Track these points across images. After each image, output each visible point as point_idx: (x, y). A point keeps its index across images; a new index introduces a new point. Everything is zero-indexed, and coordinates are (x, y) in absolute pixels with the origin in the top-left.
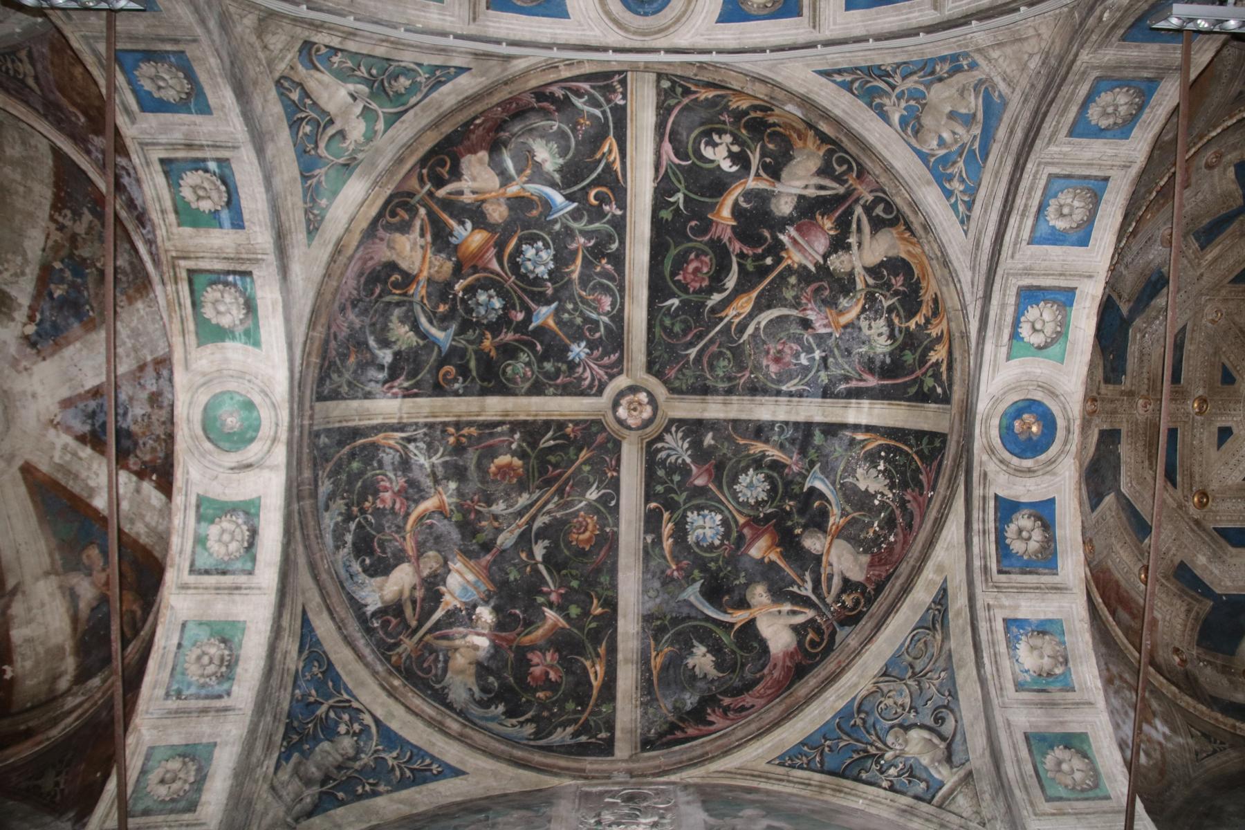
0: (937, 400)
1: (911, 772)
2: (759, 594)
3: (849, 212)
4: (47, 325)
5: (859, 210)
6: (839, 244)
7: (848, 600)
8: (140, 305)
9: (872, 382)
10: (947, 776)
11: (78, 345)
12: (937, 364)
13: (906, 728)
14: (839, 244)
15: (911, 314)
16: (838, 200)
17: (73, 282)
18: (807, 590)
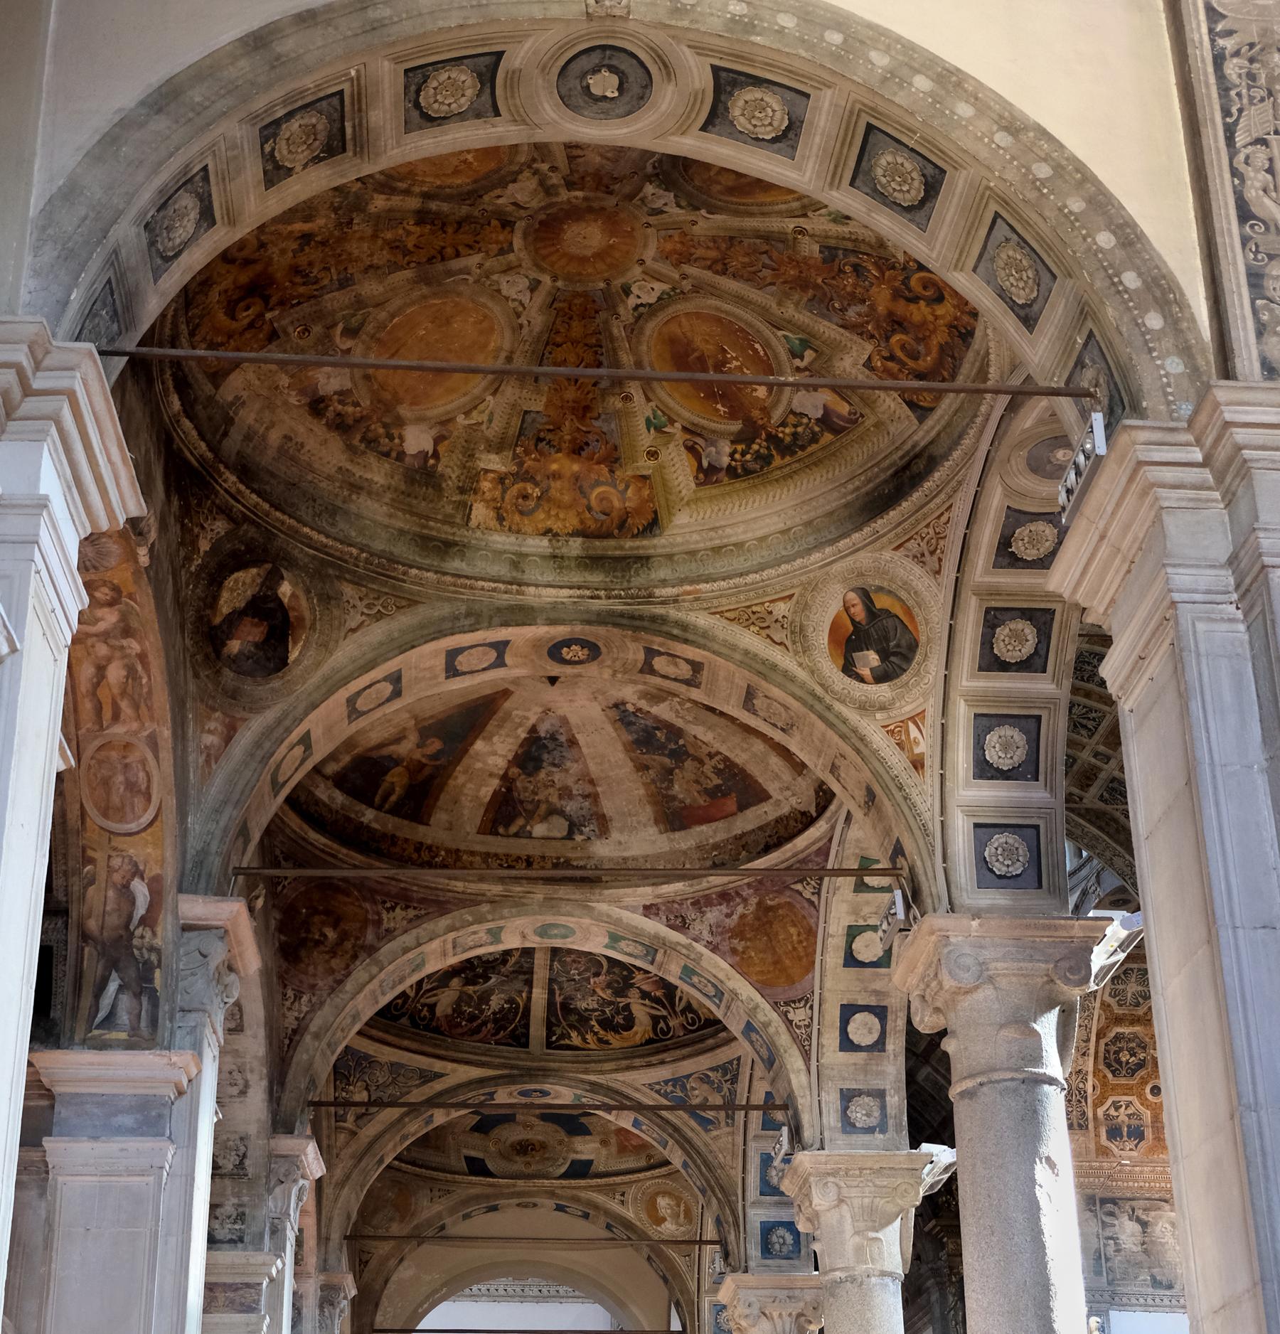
0: (548, 1037)
3: (664, 1007)
4: (633, 719)
5: (664, 1013)
6: (645, 995)
7: (425, 1012)
8: (642, 792)
9: (558, 999)
11: (614, 734)
12: (570, 1037)
13: (367, 1089)
14: (645, 995)
15: (600, 1023)
16: (673, 1005)
17: (666, 748)
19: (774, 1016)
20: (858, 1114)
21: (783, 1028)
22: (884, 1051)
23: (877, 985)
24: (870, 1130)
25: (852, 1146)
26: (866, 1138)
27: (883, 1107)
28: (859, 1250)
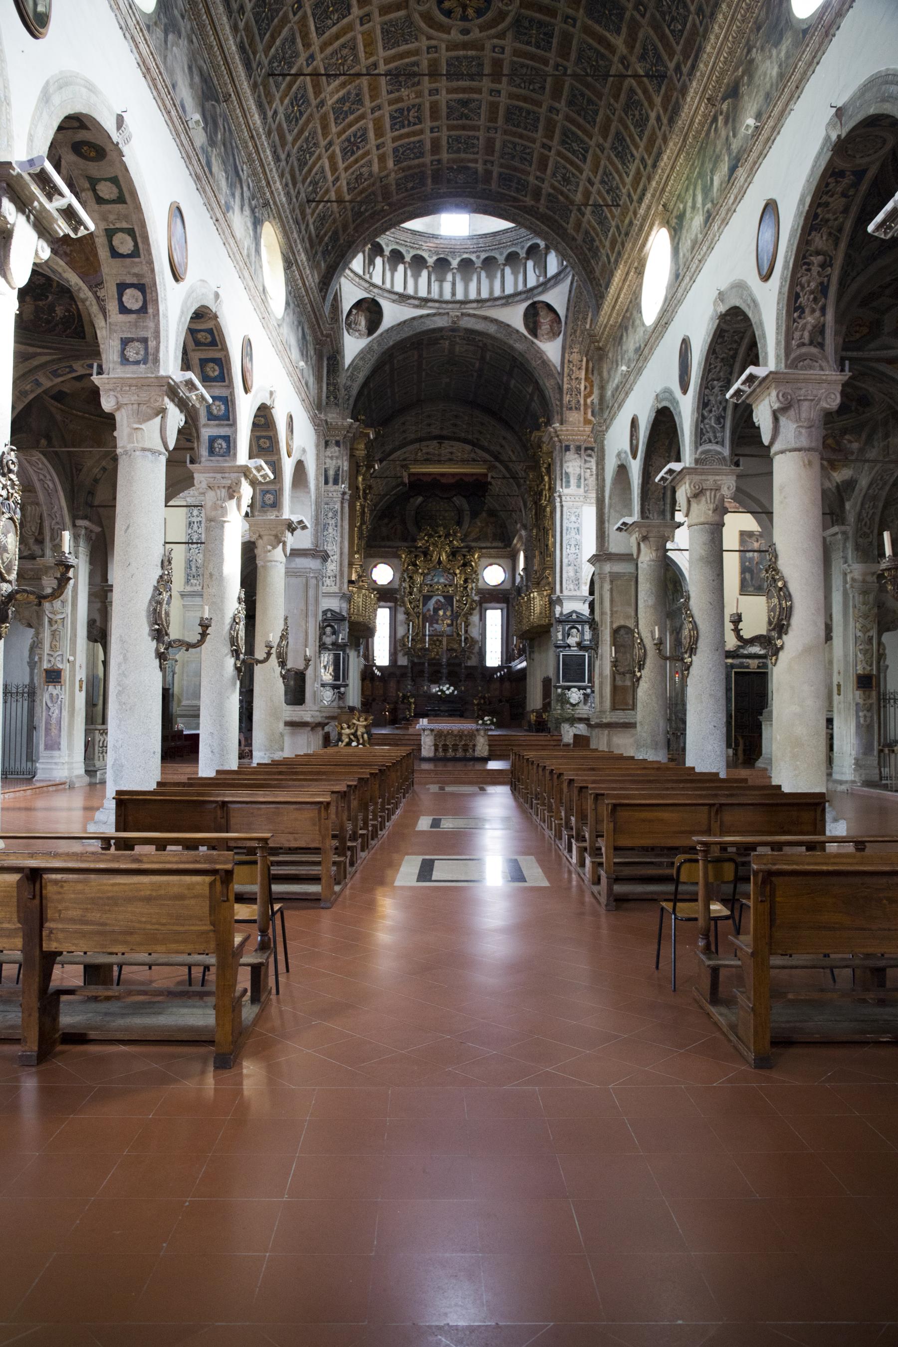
19: (90, 294)
20: (131, 354)
22: (147, 313)
23: (136, 270)
24: (137, 363)
26: (135, 367)
27: (146, 349)
28: (130, 435)
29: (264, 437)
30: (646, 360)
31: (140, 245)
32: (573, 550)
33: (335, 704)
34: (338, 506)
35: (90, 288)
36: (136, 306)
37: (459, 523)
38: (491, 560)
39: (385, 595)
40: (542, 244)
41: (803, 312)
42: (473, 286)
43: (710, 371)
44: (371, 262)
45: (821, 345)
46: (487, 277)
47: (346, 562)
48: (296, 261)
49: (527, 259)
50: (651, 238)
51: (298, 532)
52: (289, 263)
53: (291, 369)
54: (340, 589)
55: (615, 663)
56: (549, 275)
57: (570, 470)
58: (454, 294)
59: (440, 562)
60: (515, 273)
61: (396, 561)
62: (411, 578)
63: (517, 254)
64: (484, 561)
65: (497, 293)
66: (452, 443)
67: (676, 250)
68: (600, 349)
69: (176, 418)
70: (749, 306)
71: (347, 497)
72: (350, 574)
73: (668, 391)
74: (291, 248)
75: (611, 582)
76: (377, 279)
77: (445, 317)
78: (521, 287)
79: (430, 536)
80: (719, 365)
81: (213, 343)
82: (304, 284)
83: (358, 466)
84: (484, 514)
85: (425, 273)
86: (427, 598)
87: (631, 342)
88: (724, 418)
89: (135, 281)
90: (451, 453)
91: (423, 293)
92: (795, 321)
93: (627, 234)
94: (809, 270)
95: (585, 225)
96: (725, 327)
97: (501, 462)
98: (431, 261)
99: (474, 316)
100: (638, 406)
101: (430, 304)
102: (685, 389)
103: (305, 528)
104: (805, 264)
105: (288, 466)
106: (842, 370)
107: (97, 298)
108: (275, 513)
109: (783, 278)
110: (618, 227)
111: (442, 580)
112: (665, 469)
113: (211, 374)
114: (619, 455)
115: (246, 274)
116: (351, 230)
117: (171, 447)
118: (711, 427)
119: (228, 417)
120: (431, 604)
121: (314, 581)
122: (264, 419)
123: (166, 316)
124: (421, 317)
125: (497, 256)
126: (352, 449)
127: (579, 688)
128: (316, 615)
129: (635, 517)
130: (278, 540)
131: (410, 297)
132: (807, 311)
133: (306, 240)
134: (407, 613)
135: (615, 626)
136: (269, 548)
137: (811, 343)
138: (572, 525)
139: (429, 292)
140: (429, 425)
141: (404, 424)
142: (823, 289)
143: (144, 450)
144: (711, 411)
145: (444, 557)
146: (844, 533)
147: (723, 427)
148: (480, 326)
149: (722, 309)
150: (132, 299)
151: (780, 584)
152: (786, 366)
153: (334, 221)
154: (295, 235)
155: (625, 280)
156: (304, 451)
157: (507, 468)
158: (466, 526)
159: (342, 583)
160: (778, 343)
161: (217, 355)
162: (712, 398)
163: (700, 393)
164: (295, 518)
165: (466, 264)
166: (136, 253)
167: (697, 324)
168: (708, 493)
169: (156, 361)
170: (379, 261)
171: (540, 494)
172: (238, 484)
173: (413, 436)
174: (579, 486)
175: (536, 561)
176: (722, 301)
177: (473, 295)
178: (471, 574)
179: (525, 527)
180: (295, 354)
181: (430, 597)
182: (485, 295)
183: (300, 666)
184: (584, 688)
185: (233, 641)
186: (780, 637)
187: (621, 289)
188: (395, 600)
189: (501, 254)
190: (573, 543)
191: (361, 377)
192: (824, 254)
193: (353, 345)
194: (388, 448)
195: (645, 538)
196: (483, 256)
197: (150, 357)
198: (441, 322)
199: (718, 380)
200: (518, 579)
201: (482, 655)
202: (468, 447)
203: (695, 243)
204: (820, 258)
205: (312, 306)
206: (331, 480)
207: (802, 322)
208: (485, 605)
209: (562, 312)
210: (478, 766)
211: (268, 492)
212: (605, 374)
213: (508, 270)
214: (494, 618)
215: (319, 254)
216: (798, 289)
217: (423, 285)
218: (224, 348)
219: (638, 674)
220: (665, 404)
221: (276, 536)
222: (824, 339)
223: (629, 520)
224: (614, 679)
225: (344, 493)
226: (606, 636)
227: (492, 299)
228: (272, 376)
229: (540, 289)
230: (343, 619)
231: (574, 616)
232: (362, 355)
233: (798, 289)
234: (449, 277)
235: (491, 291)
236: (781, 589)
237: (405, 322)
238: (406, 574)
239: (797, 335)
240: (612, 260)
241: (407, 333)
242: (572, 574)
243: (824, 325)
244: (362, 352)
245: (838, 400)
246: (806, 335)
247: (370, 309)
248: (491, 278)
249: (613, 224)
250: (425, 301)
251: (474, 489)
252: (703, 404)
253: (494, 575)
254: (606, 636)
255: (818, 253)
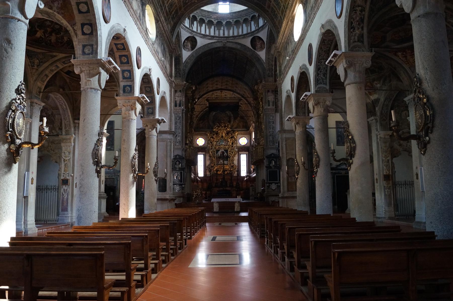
1: (34, 63)
2: (42, 31)
7: (49, 42)
10: (36, 67)
13: (38, 59)
18: (47, 36)
19: (71, 28)
21: (73, 31)
24: (89, 54)
25: (84, 58)
27: (93, 49)
28: (86, 83)
29: (148, 87)
30: (296, 54)
31: (90, 8)
32: (272, 130)
33: (180, 191)
34: (181, 115)
35: (71, 26)
36: (88, 32)
37: (230, 122)
38: (242, 136)
39: (202, 149)
40: (257, 15)
41: (354, 29)
42: (231, 32)
43: (320, 56)
44: (192, 23)
45: (362, 42)
46: (237, 28)
47: (184, 137)
48: (160, 20)
49: (251, 21)
50: (296, 8)
51: (162, 124)
52: (157, 21)
53: (158, 61)
54: (182, 147)
55: (288, 173)
56: (260, 26)
57: (270, 99)
58: (224, 34)
59: (222, 137)
60: (247, 26)
61: (205, 136)
62: (211, 143)
63: (248, 19)
64: (239, 136)
65: (240, 33)
66: (226, 91)
67: (305, 11)
68: (278, 52)
69: (105, 76)
70: (333, 29)
71: (184, 111)
72: (186, 141)
73: (304, 65)
74: (158, 15)
75: (286, 141)
76: (195, 29)
77: (221, 43)
78: (249, 31)
79: (219, 127)
80: (323, 53)
81: (124, 49)
82: (164, 29)
83: (189, 100)
84: (239, 118)
85: (213, 27)
86: (218, 151)
87: (290, 49)
88: (326, 74)
89: (88, 22)
90: (226, 95)
91: (212, 34)
92: (351, 33)
93: (287, 8)
94: (356, 13)
95: (271, 6)
96: (324, 38)
97: (245, 98)
98: (215, 22)
99: (232, 42)
100: (293, 72)
101: (215, 38)
102: (310, 64)
103: (164, 122)
104: (354, 10)
105: (158, 98)
106: (371, 51)
107: (74, 29)
108: (153, 116)
109: (346, 16)
110: (284, 6)
111: (223, 144)
112: (304, 95)
113: (124, 61)
114: (287, 92)
115: (138, 23)
116: (183, 9)
117: (103, 87)
118: (322, 78)
119: (131, 78)
120: (219, 153)
121: (169, 143)
122: (146, 79)
123: (101, 36)
124: (212, 43)
125: (240, 20)
126: (186, 93)
127: (276, 183)
128: (171, 157)
129: (294, 115)
130: (154, 127)
131: (207, 36)
132: (356, 28)
133: (165, 13)
134: (210, 157)
135: (288, 158)
136: (150, 130)
137: (359, 41)
138: (271, 120)
139: (215, 34)
140: (217, 85)
141: (207, 84)
142: (362, 20)
143: (91, 88)
144: (321, 72)
145: (224, 135)
146: (376, 119)
147: (326, 78)
148: (234, 46)
149: (323, 31)
150: (87, 29)
151: (350, 137)
152: (349, 51)
153: (176, 6)
154: (159, 10)
155: (287, 25)
156: (165, 93)
157: (247, 100)
158: (232, 123)
159: (182, 144)
160: (345, 41)
161: (126, 54)
162: (321, 67)
163: (316, 65)
164: (160, 118)
165: (229, 24)
166: (88, 11)
167: (314, 38)
168: (321, 104)
169: (97, 53)
170: (195, 23)
171: (259, 109)
172: (135, 104)
173: (211, 89)
174: (273, 106)
175: (258, 135)
176: (323, 28)
177: (231, 34)
178: (235, 141)
179: (254, 122)
180: (160, 55)
181: (219, 150)
182: (236, 34)
183: (163, 176)
184: (277, 183)
185: (133, 166)
186: (351, 159)
187: (286, 28)
188: (205, 151)
189: (242, 19)
190: (271, 127)
191: (189, 66)
192: (361, 6)
193: (186, 54)
194: (201, 94)
195: (298, 123)
196: (235, 20)
197: (94, 52)
198: (219, 45)
199: (323, 59)
200: (252, 142)
201: (239, 171)
202: (232, 93)
203: (312, 8)
204: (360, 8)
205: (167, 37)
206: (178, 105)
207: (354, 33)
208: (240, 153)
209: (265, 40)
210: (236, 215)
211: (150, 108)
212: (281, 61)
213: (244, 25)
214: (244, 158)
215: (171, 18)
216: (352, 20)
217: (212, 31)
218: (129, 51)
219: (297, 177)
220: (303, 70)
221: (153, 125)
222: (363, 39)
223: (291, 116)
224: (288, 179)
225: (183, 110)
226: (284, 162)
227: (239, 36)
228: (149, 63)
229: (256, 32)
230: (183, 158)
231: (273, 155)
232: (189, 58)
233: (352, 20)
234: (222, 28)
235: (238, 32)
236: (351, 139)
237: (205, 45)
238: (208, 141)
239: (352, 38)
240: (282, 18)
241: (207, 49)
242: (271, 139)
243: (363, 34)
244: (189, 56)
245: (371, 63)
246: (356, 38)
247: (192, 40)
248: (238, 29)
249: (282, 4)
250: (213, 37)
251: (234, 108)
252: (318, 69)
253: (243, 141)
254: (284, 162)
255: (359, 6)
